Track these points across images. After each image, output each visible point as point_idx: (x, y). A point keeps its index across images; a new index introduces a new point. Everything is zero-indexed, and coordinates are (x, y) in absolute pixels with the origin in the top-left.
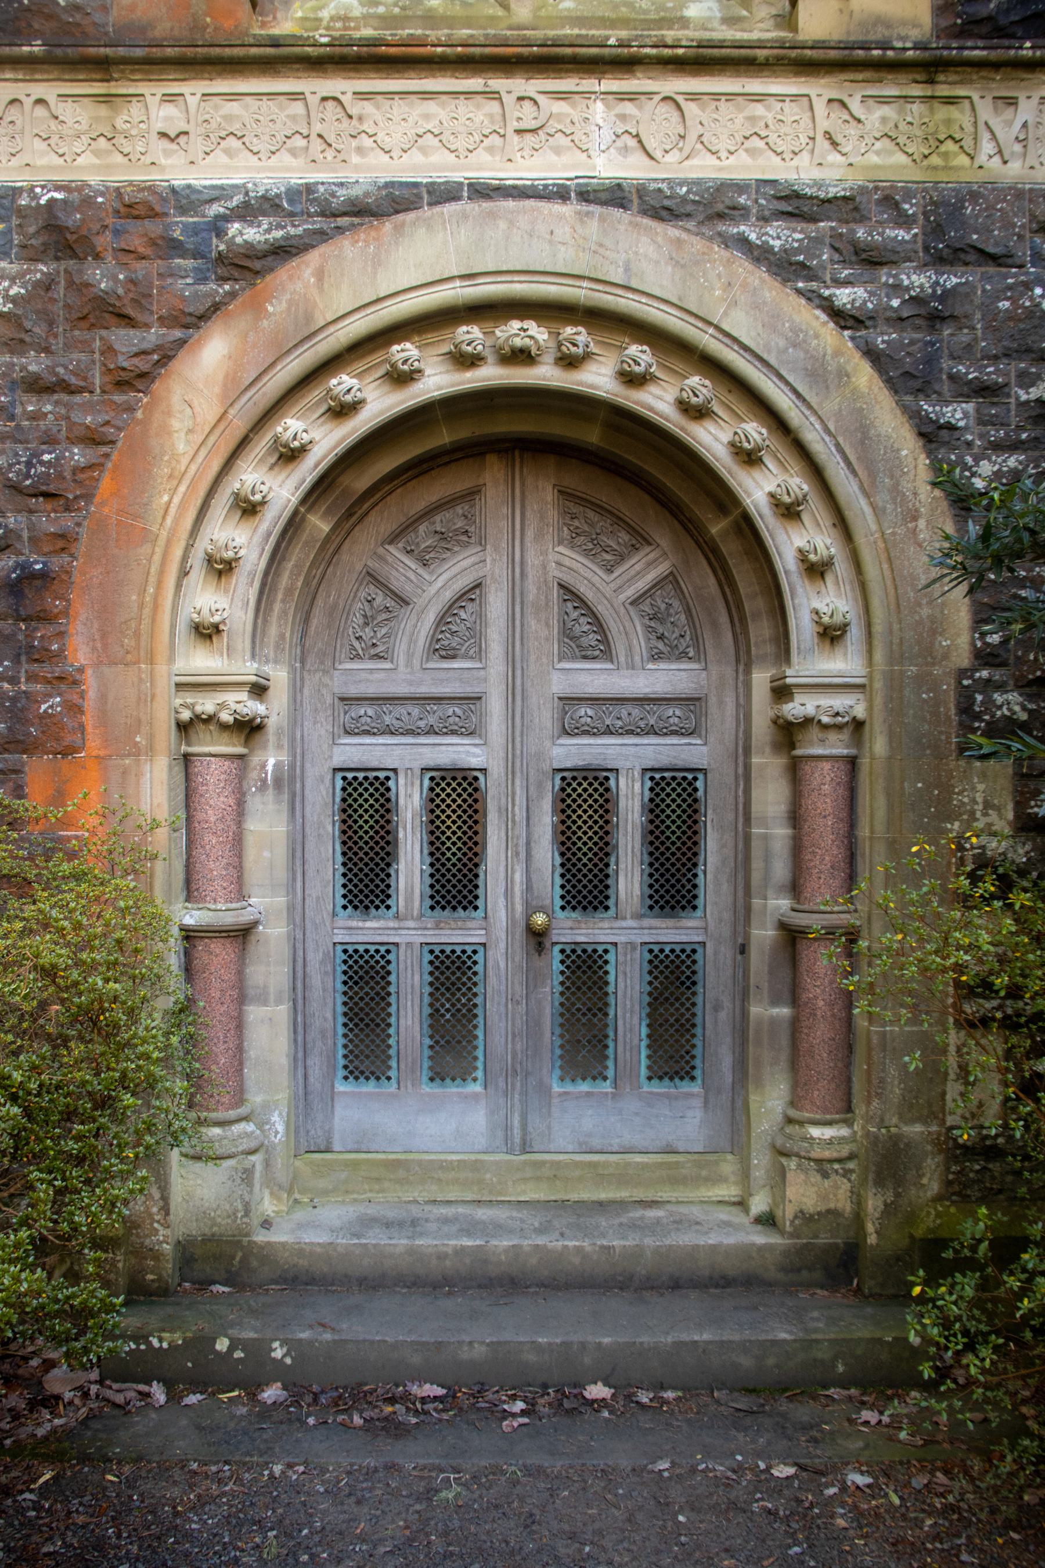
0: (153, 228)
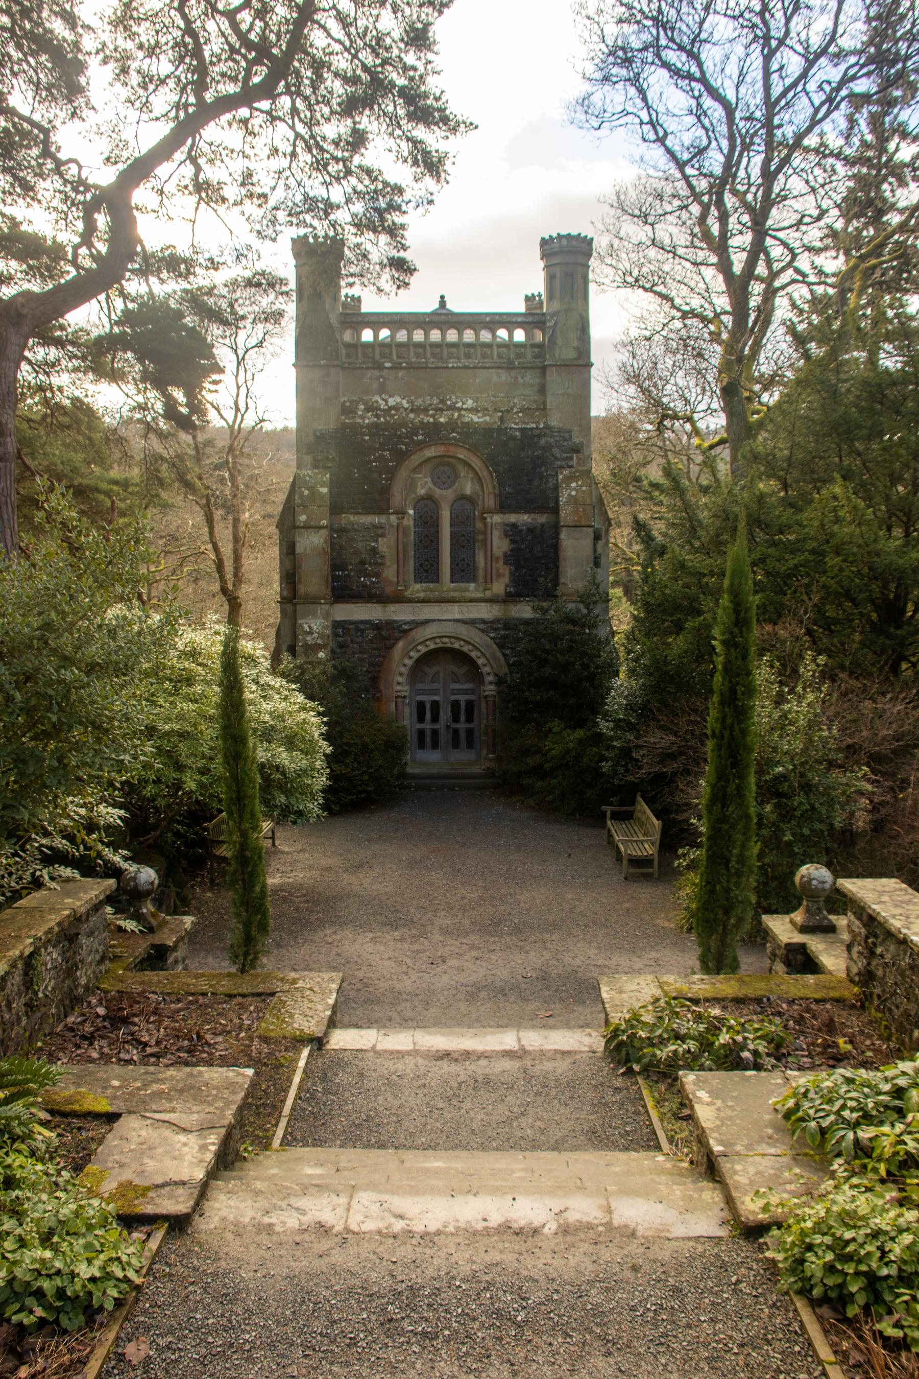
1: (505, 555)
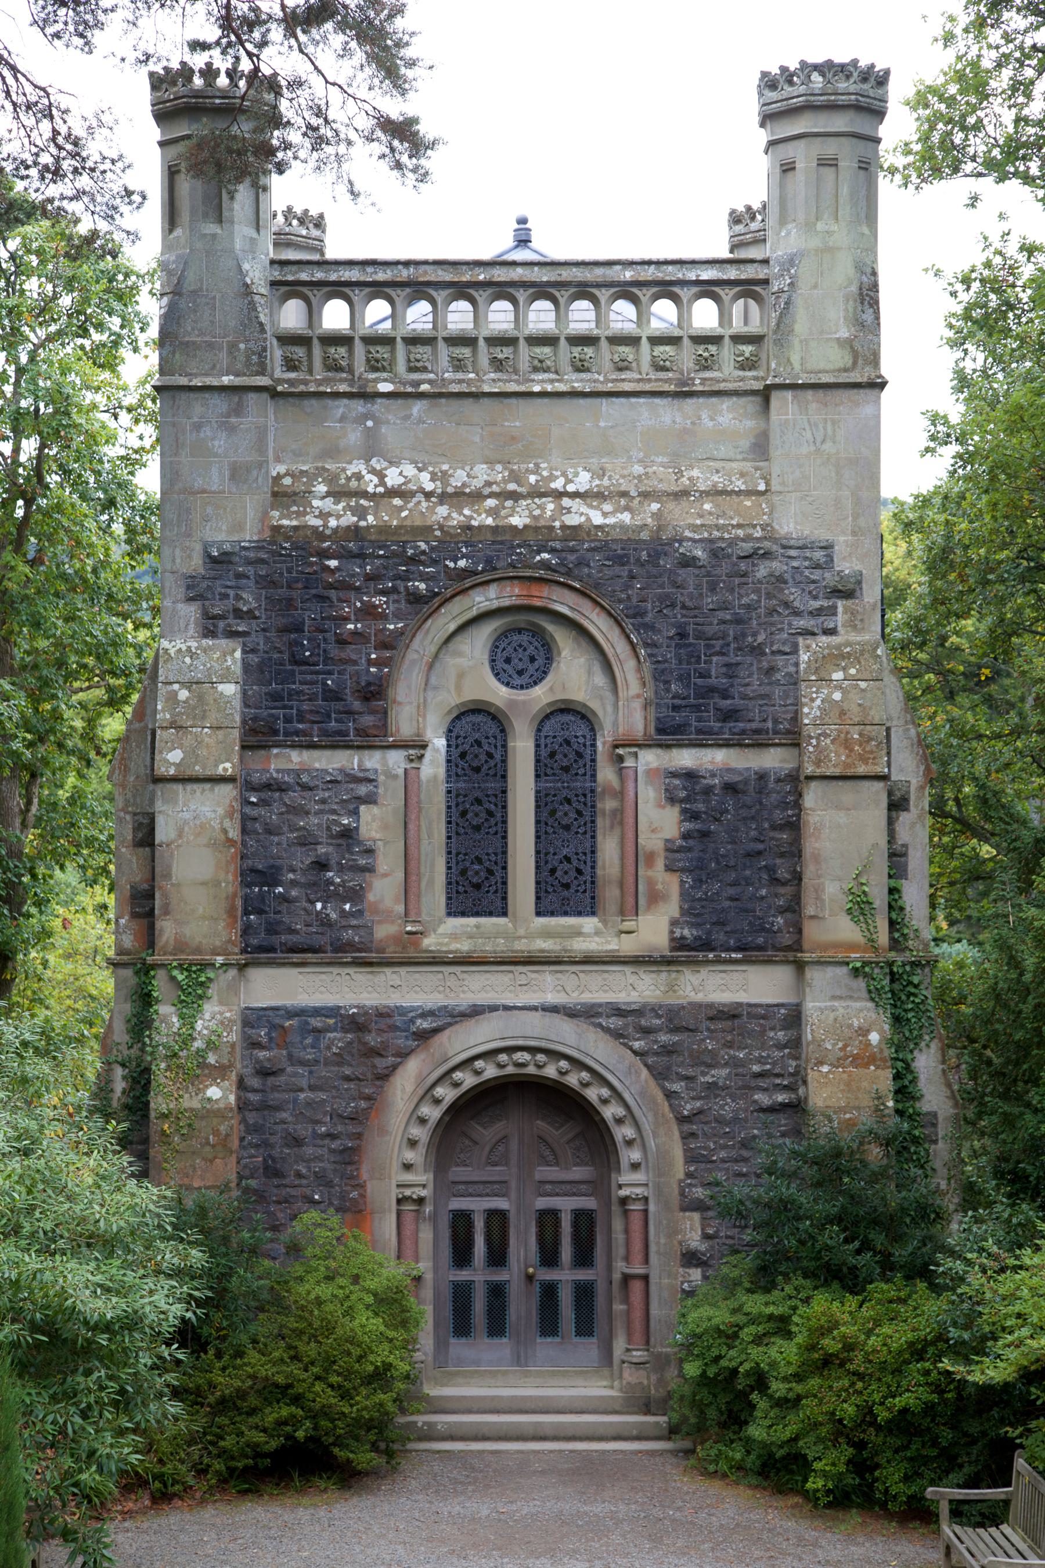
0: (389, 1021)
1: (670, 848)
